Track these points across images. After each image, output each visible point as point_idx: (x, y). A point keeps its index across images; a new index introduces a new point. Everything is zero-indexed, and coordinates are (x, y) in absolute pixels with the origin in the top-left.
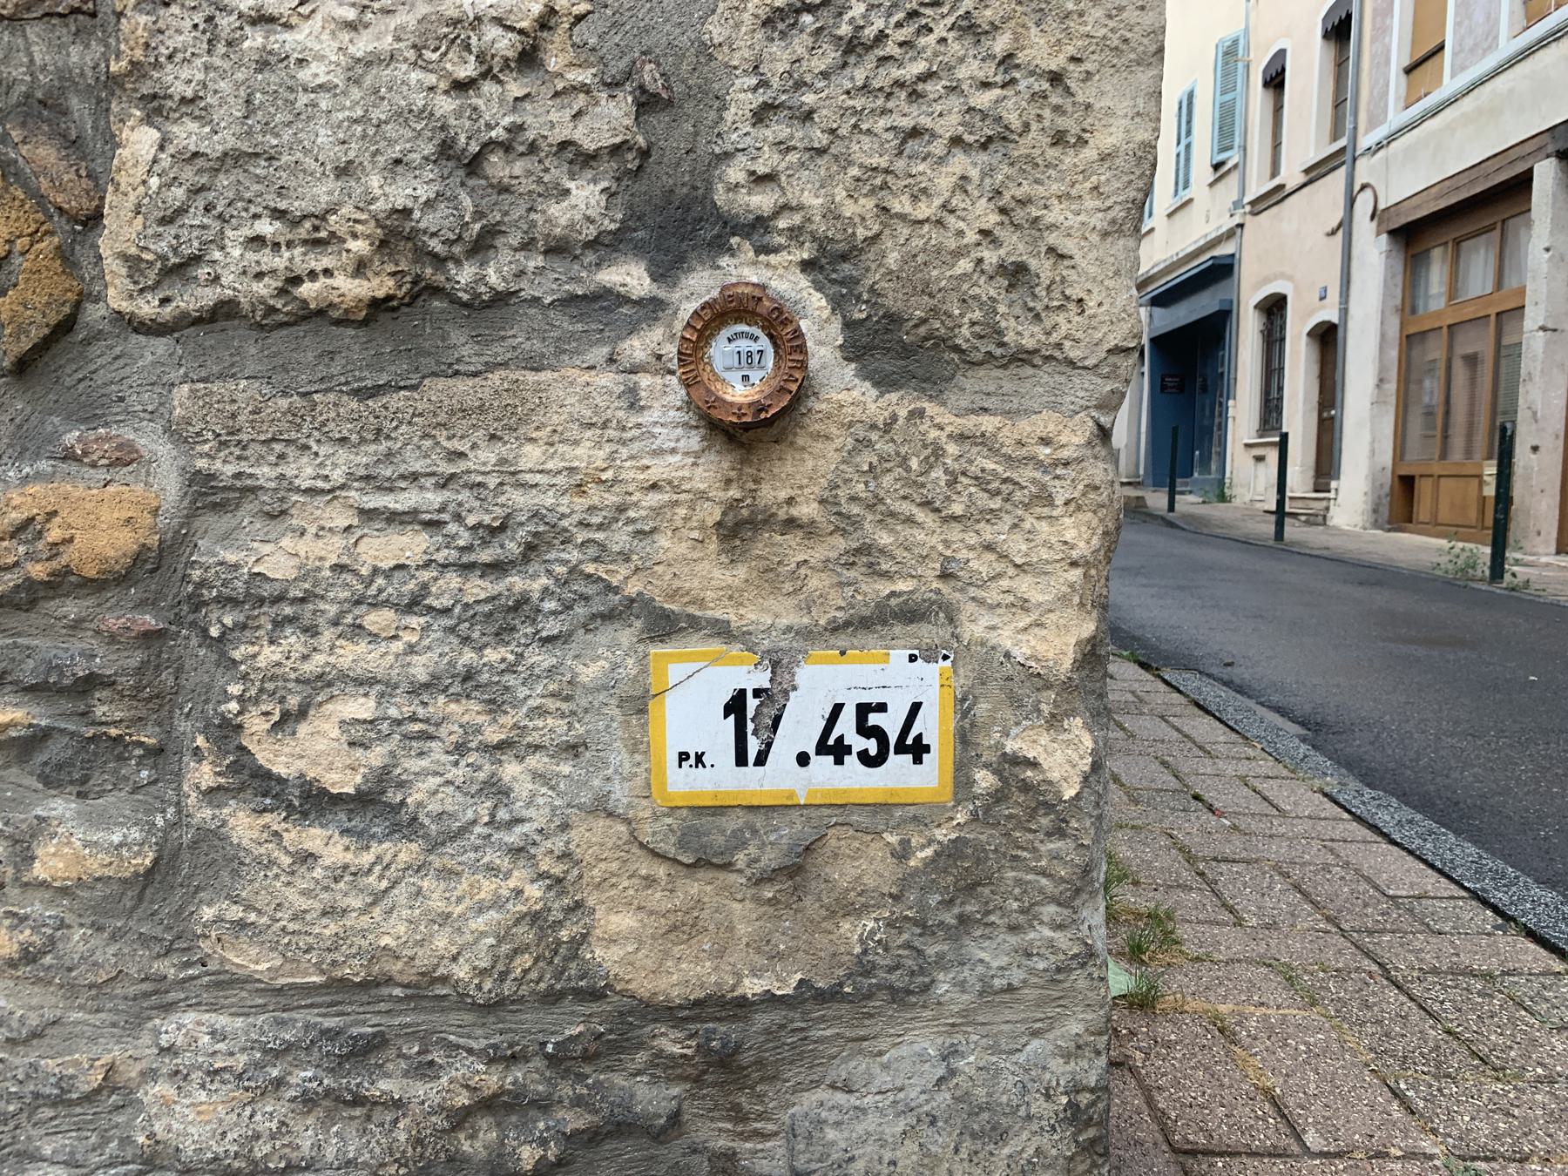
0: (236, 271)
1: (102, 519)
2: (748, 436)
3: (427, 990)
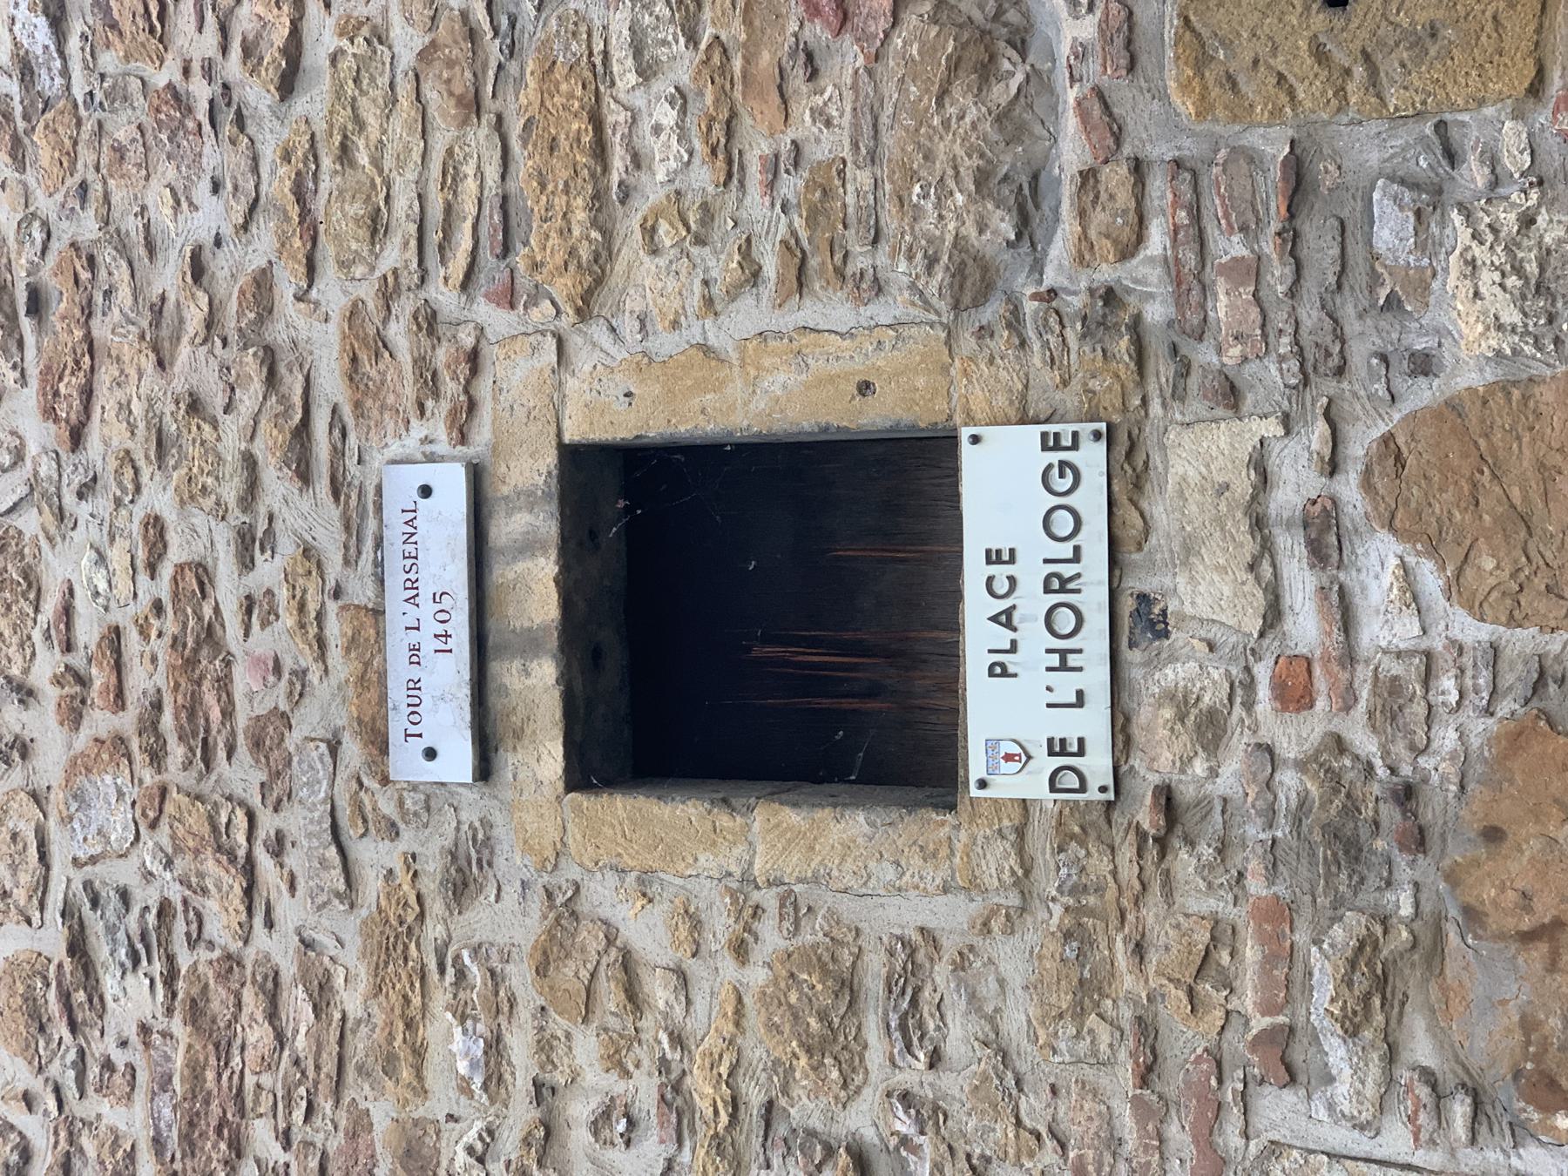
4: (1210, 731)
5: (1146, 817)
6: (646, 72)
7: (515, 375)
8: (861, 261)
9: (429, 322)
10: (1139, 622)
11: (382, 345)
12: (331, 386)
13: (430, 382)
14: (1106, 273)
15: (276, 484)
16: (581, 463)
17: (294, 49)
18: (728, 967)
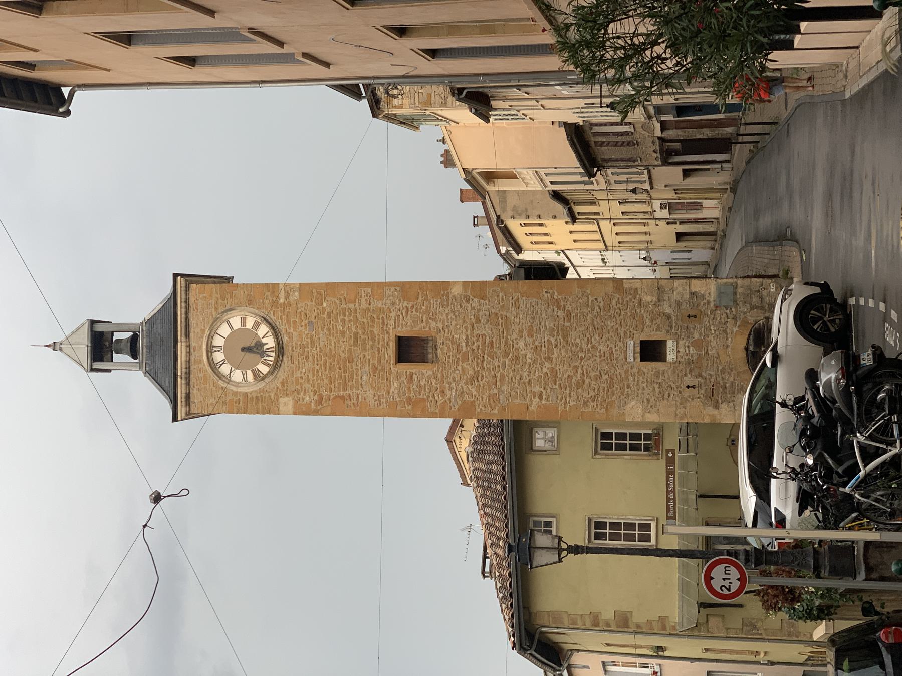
7: (636, 336)
10: (678, 351)
12: (622, 335)
16: (641, 341)
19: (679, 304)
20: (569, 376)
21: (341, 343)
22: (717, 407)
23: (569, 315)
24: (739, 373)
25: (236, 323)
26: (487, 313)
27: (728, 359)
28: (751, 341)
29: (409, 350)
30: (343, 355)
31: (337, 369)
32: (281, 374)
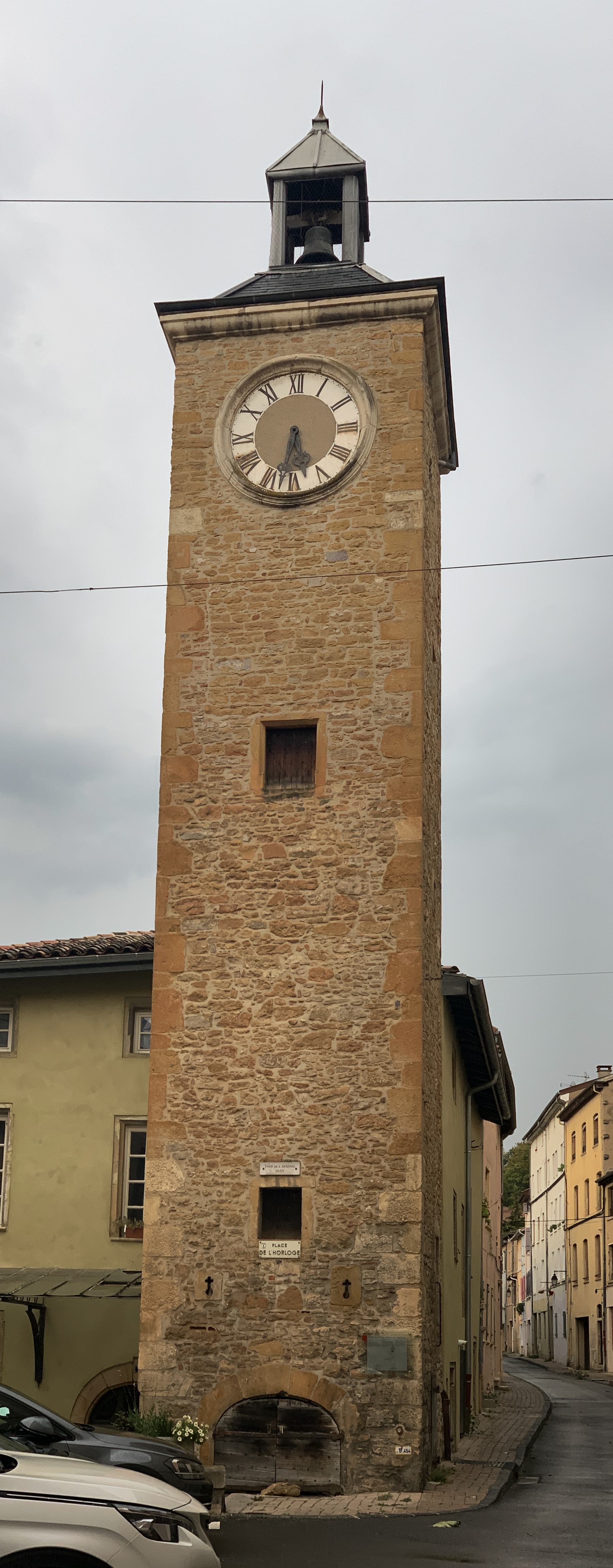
0: (373, 1425)
1: (366, 1438)
2: (400, 1434)
3: (382, 1465)
4: (267, 1269)
5: (257, 1261)
6: (346, 1200)
7: (310, 1181)
8: (321, 1228)
9: (318, 1168)
10: (279, 1261)
11: (315, 1161)
12: (312, 1153)
13: (310, 1168)
14: (317, 1258)
15: (298, 1144)
17: (354, 1148)
18: (239, 1209)
19: (371, 1264)
20: (234, 1050)
21: (304, 616)
22: (170, 1335)
23: (353, 1047)
24: (233, 1379)
25: (347, 414)
26: (358, 890)
27: (262, 1358)
28: (296, 1405)
29: (290, 747)
30: (282, 620)
31: (253, 613)
32: (246, 508)
